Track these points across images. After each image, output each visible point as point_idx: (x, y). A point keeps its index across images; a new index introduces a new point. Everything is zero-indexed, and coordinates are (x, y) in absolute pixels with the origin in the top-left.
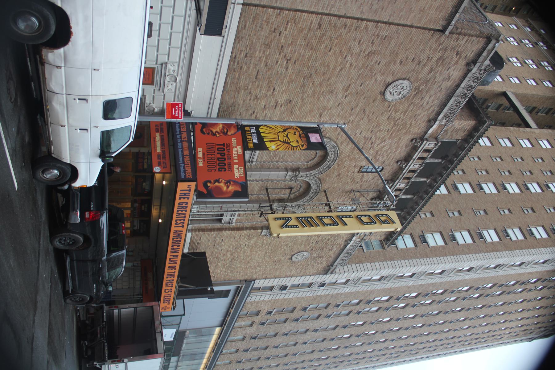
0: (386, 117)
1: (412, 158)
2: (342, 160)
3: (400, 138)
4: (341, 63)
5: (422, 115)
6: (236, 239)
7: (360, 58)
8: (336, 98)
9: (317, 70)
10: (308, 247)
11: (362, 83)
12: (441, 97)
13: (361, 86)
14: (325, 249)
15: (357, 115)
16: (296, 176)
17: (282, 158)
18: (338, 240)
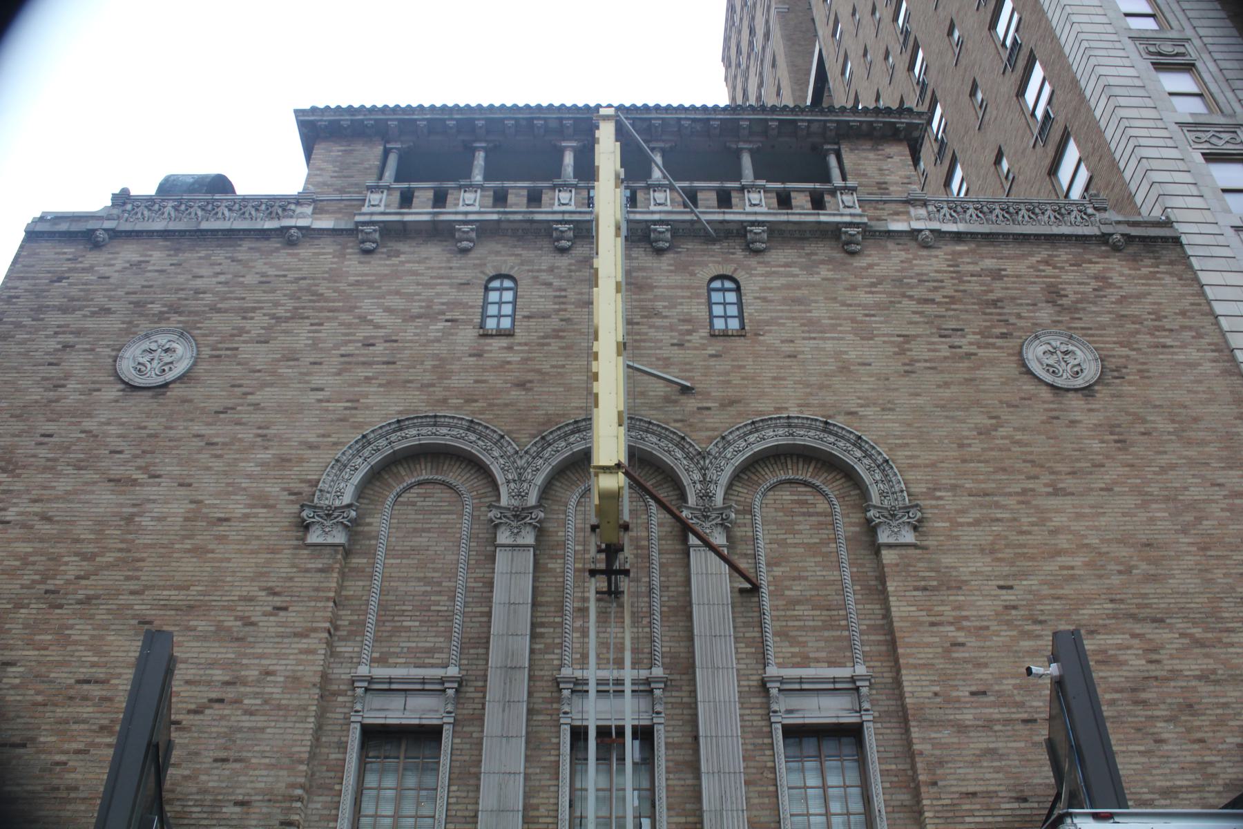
0: (263, 347)
1: (434, 222)
2: (445, 401)
3: (357, 283)
4: (24, 526)
5: (265, 269)
6: (961, 637)
7: (18, 486)
8: (154, 501)
9: (34, 582)
10: (982, 353)
11: (111, 452)
12: (202, 254)
13: (120, 452)
14: (991, 296)
15: (238, 423)
16: (519, 514)
17: (439, 584)
18: (925, 270)
